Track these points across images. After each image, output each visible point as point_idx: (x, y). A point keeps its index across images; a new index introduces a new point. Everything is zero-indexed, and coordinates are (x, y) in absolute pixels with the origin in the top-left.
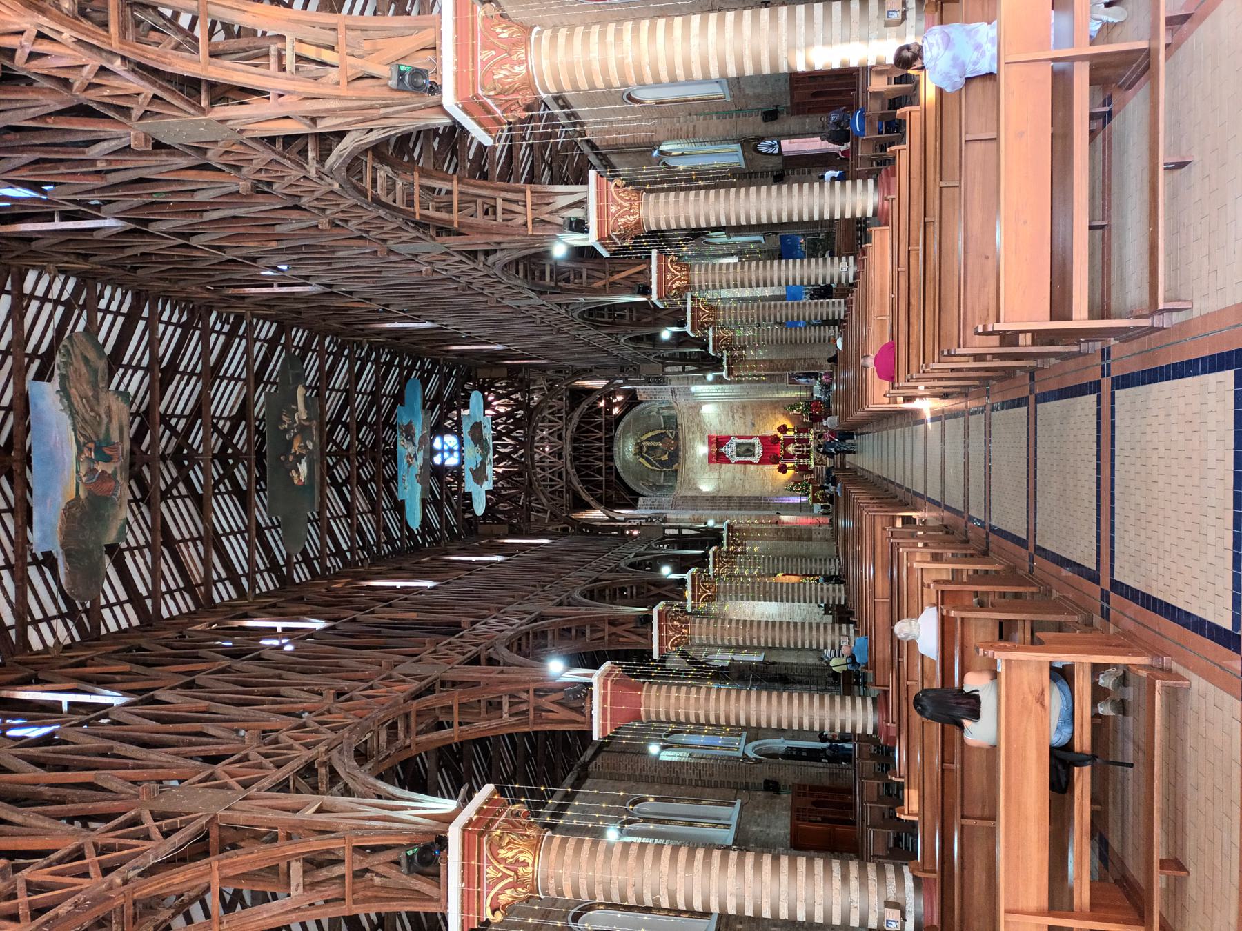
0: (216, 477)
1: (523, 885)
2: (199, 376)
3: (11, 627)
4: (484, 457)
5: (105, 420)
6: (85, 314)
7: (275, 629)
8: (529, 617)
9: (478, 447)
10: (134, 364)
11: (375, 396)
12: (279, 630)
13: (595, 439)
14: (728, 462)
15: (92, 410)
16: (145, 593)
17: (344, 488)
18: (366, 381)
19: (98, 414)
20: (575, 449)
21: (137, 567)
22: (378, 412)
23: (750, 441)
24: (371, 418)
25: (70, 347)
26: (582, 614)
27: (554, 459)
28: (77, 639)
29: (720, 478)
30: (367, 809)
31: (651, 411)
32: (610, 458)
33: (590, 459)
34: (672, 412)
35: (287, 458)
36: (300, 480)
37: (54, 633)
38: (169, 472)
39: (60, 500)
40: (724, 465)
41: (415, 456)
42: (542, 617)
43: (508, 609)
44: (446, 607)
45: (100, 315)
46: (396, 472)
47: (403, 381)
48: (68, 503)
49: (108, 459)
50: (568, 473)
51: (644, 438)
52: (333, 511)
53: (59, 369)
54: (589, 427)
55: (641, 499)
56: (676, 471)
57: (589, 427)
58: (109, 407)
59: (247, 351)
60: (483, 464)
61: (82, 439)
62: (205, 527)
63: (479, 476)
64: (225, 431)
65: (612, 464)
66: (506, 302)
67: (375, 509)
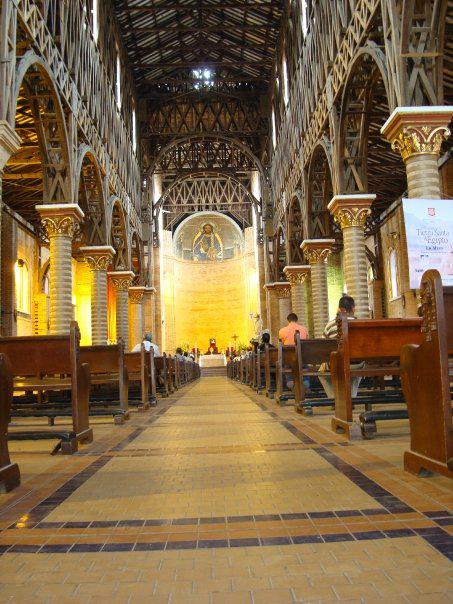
8: (67, 99)
26: (70, 145)
32: (200, 209)
42: (68, 112)
43: (74, 86)
44: (74, 35)
54: (223, 193)
65: (196, 210)
66: (329, 79)
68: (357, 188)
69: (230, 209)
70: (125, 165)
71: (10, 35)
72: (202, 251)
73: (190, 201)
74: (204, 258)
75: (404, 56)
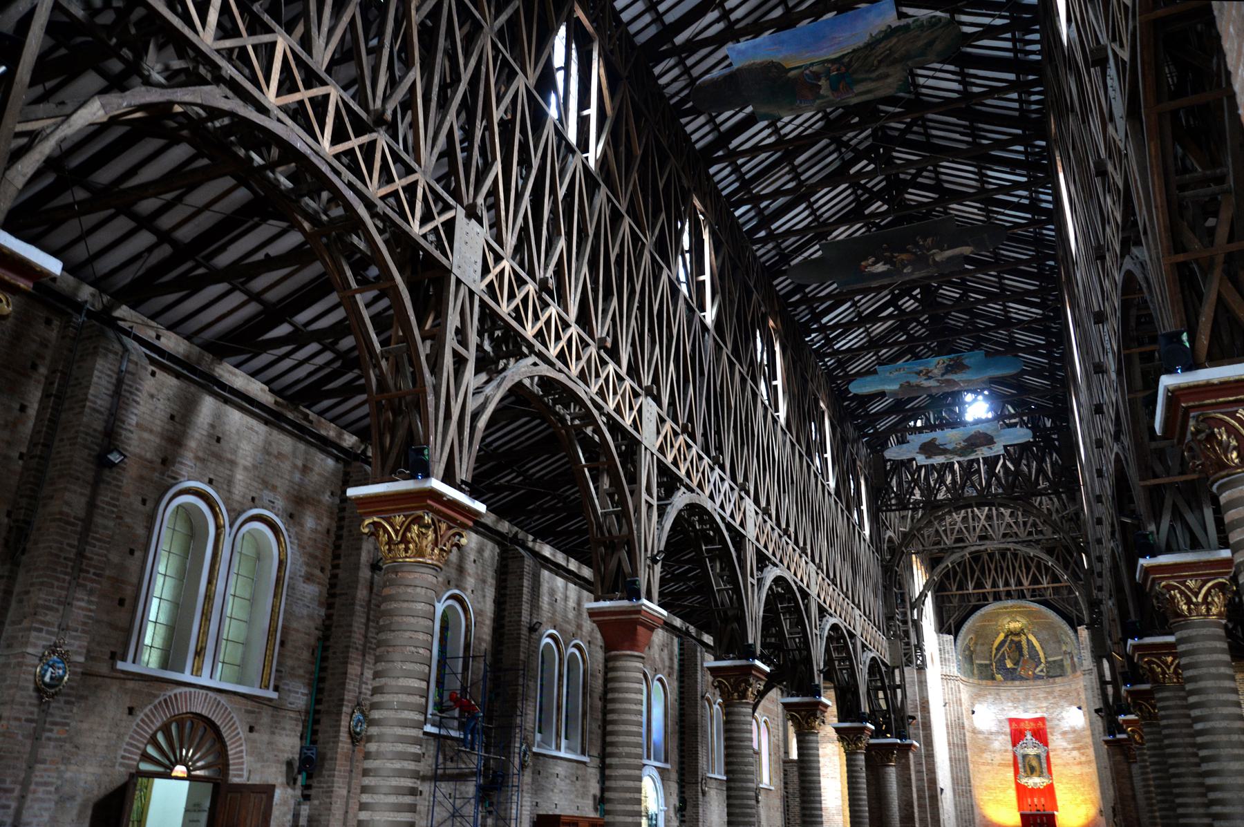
0: (869, 185)
1: (390, 550)
2: (974, 144)
3: (673, 43)
4: (954, 452)
5: (874, 75)
6: (1008, 21)
9: (963, 444)
10: (968, 79)
11: (1007, 322)
13: (1006, 578)
14: (1014, 745)
15: (880, 62)
16: (732, 146)
17: (891, 309)
18: (1019, 311)
19: (877, 68)
20: (991, 555)
21: (760, 133)
22: (988, 328)
23: (1045, 770)
24: (982, 323)
25: (941, 25)
27: (978, 530)
28: (672, 102)
29: (991, 733)
30: (460, 400)
31: (1066, 644)
32: (997, 597)
33: (993, 572)
34: (1069, 670)
35: (886, 250)
36: (866, 267)
37: (675, 80)
38: (860, 138)
39: (781, 56)
40: (1009, 738)
41: (930, 378)
43: (749, 503)
45: (1008, 35)
46: (920, 358)
47: (1033, 349)
48: (779, 64)
49: (834, 88)
50: (962, 548)
51: (1031, 637)
52: (863, 301)
53: (914, 22)
54: (1033, 569)
55: (952, 637)
56: (993, 678)
57: (1033, 569)
58: (887, 76)
59: (1017, 185)
60: (944, 452)
61: (846, 60)
62: (812, 185)
63: (929, 449)
64: (920, 180)
65: (991, 599)
67: (873, 344)
69: (1049, 595)
70: (847, 566)
71: (649, 492)
72: (1009, 665)
73: (979, 585)
75: (1142, 483)
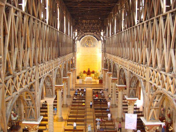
7: (46, 7)
12: (46, 8)
32: (87, 35)
68: (122, 84)
72: (87, 44)
74: (87, 46)
